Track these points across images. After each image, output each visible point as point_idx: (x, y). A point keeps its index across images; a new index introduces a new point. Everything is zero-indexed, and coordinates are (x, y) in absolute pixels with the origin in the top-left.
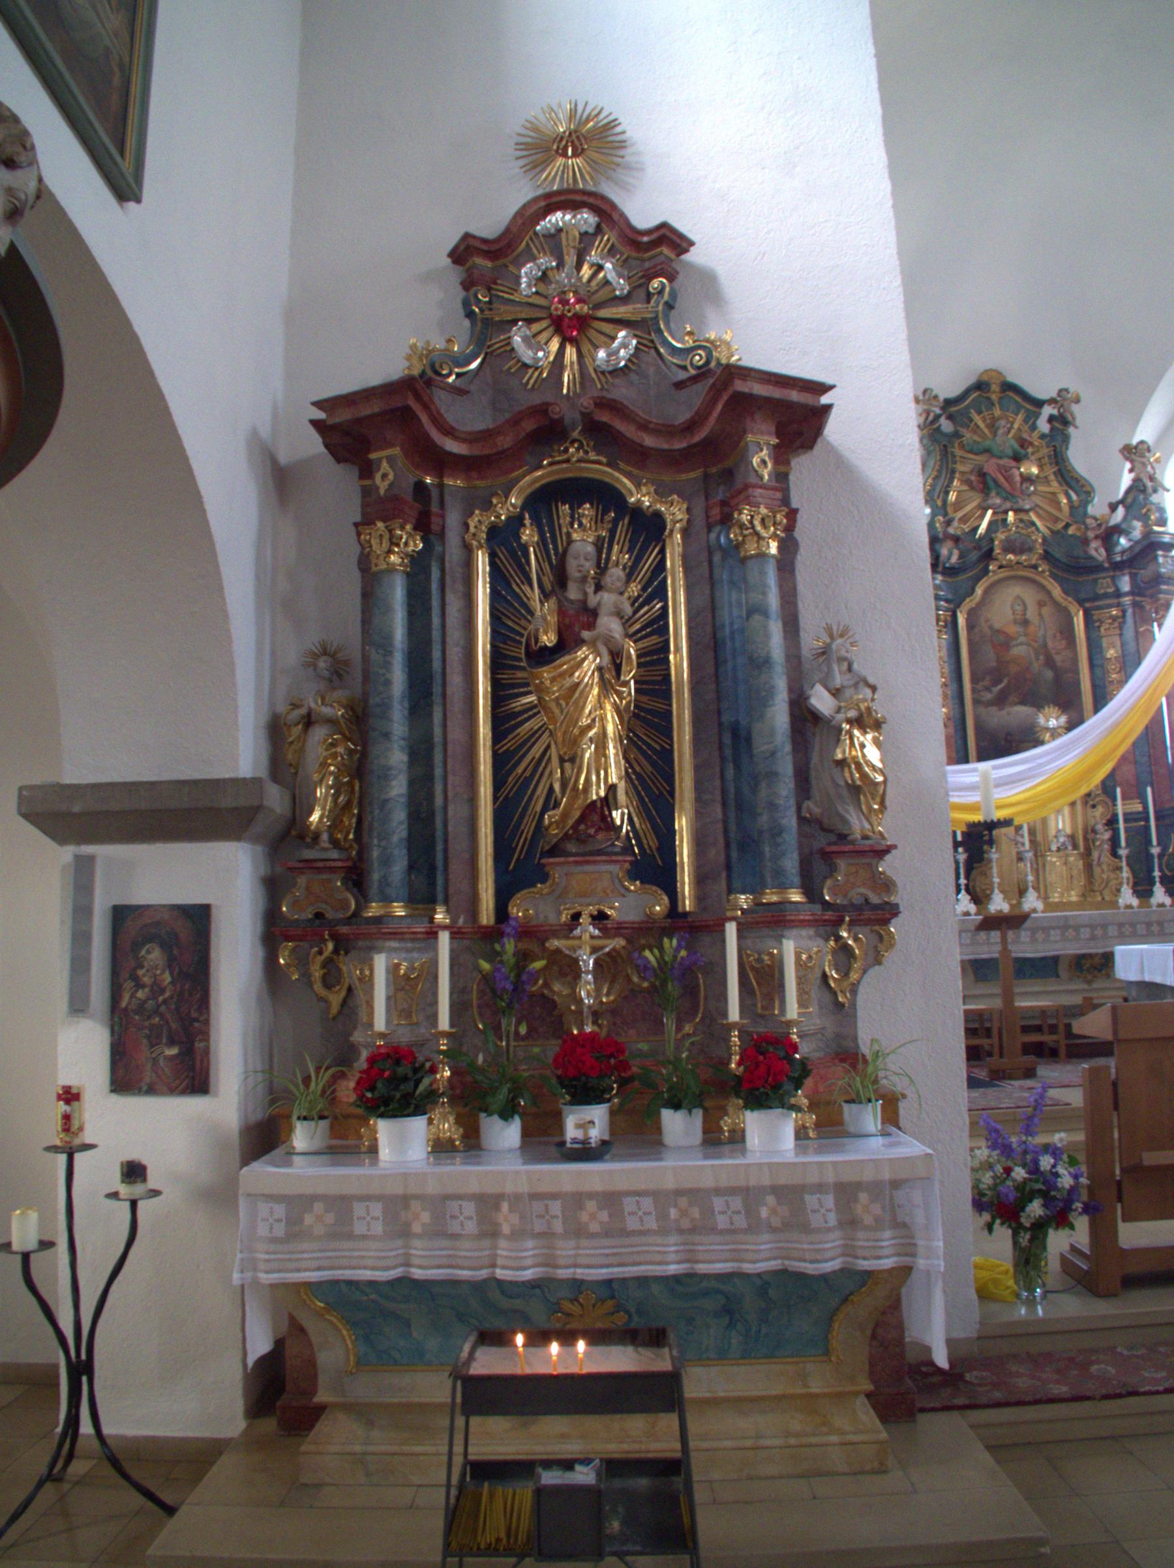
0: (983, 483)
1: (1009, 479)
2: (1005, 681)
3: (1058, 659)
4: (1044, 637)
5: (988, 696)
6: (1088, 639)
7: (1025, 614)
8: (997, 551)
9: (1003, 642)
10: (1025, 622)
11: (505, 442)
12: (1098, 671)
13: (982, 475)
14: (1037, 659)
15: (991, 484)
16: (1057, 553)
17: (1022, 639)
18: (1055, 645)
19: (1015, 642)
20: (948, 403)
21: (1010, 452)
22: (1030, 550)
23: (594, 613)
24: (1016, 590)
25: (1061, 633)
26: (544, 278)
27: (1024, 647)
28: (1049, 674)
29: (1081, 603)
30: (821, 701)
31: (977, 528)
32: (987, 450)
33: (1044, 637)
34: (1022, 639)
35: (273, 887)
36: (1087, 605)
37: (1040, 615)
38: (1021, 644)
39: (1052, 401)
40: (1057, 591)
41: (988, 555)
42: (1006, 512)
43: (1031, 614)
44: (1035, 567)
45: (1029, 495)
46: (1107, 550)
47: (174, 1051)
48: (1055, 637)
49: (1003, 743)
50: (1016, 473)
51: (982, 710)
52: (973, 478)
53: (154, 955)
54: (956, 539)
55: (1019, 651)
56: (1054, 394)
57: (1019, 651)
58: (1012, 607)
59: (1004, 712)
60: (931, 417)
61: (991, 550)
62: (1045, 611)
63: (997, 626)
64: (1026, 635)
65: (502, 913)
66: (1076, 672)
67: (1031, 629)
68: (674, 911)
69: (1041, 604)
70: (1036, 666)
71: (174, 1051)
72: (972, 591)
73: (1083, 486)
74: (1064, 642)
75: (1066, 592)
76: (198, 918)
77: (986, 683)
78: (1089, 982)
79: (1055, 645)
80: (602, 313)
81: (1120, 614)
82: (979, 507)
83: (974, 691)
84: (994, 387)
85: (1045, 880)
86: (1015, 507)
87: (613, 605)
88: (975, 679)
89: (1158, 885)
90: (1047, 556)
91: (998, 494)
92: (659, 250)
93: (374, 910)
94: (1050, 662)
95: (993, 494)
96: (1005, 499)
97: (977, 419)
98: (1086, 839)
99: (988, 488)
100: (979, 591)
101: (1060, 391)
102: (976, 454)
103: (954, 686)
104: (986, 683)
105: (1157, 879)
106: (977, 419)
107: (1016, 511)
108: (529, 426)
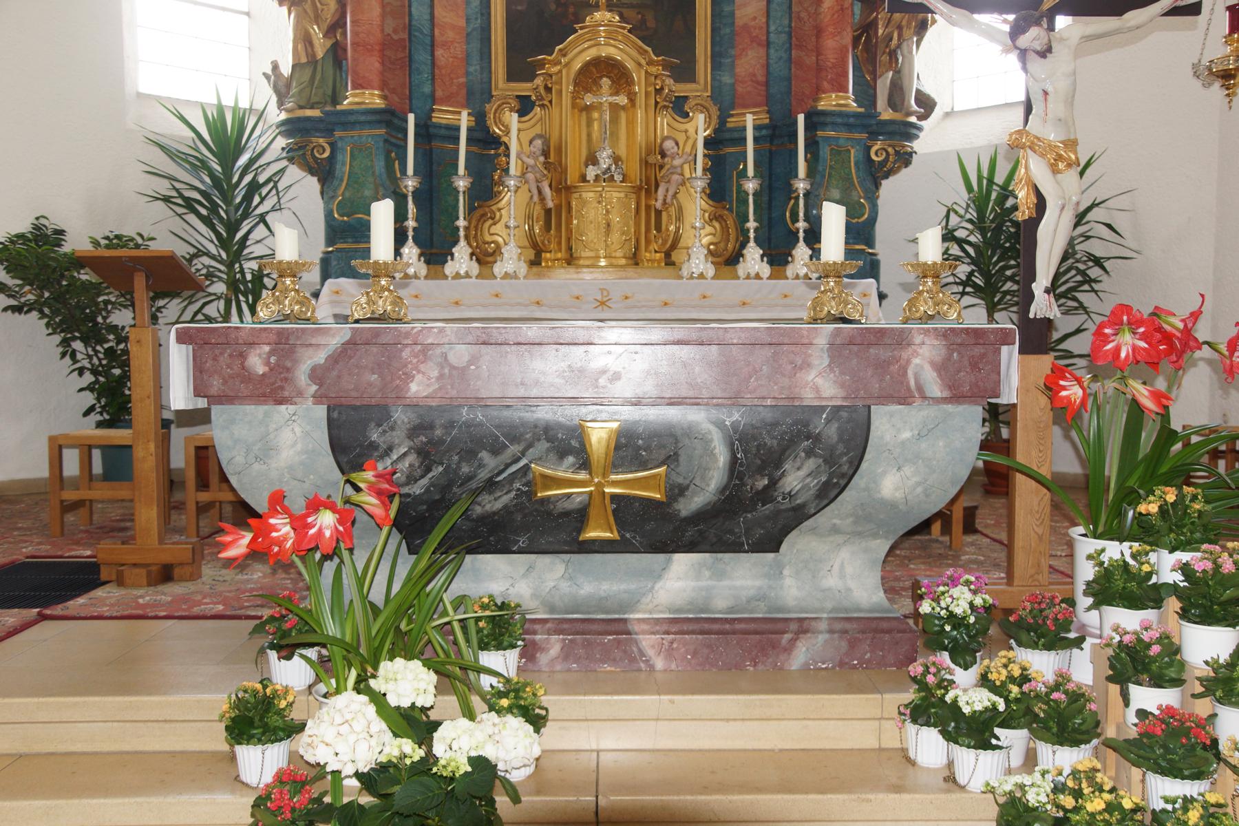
49: (553, 7)
85: (569, 231)
89: (752, 244)
98: (645, 164)
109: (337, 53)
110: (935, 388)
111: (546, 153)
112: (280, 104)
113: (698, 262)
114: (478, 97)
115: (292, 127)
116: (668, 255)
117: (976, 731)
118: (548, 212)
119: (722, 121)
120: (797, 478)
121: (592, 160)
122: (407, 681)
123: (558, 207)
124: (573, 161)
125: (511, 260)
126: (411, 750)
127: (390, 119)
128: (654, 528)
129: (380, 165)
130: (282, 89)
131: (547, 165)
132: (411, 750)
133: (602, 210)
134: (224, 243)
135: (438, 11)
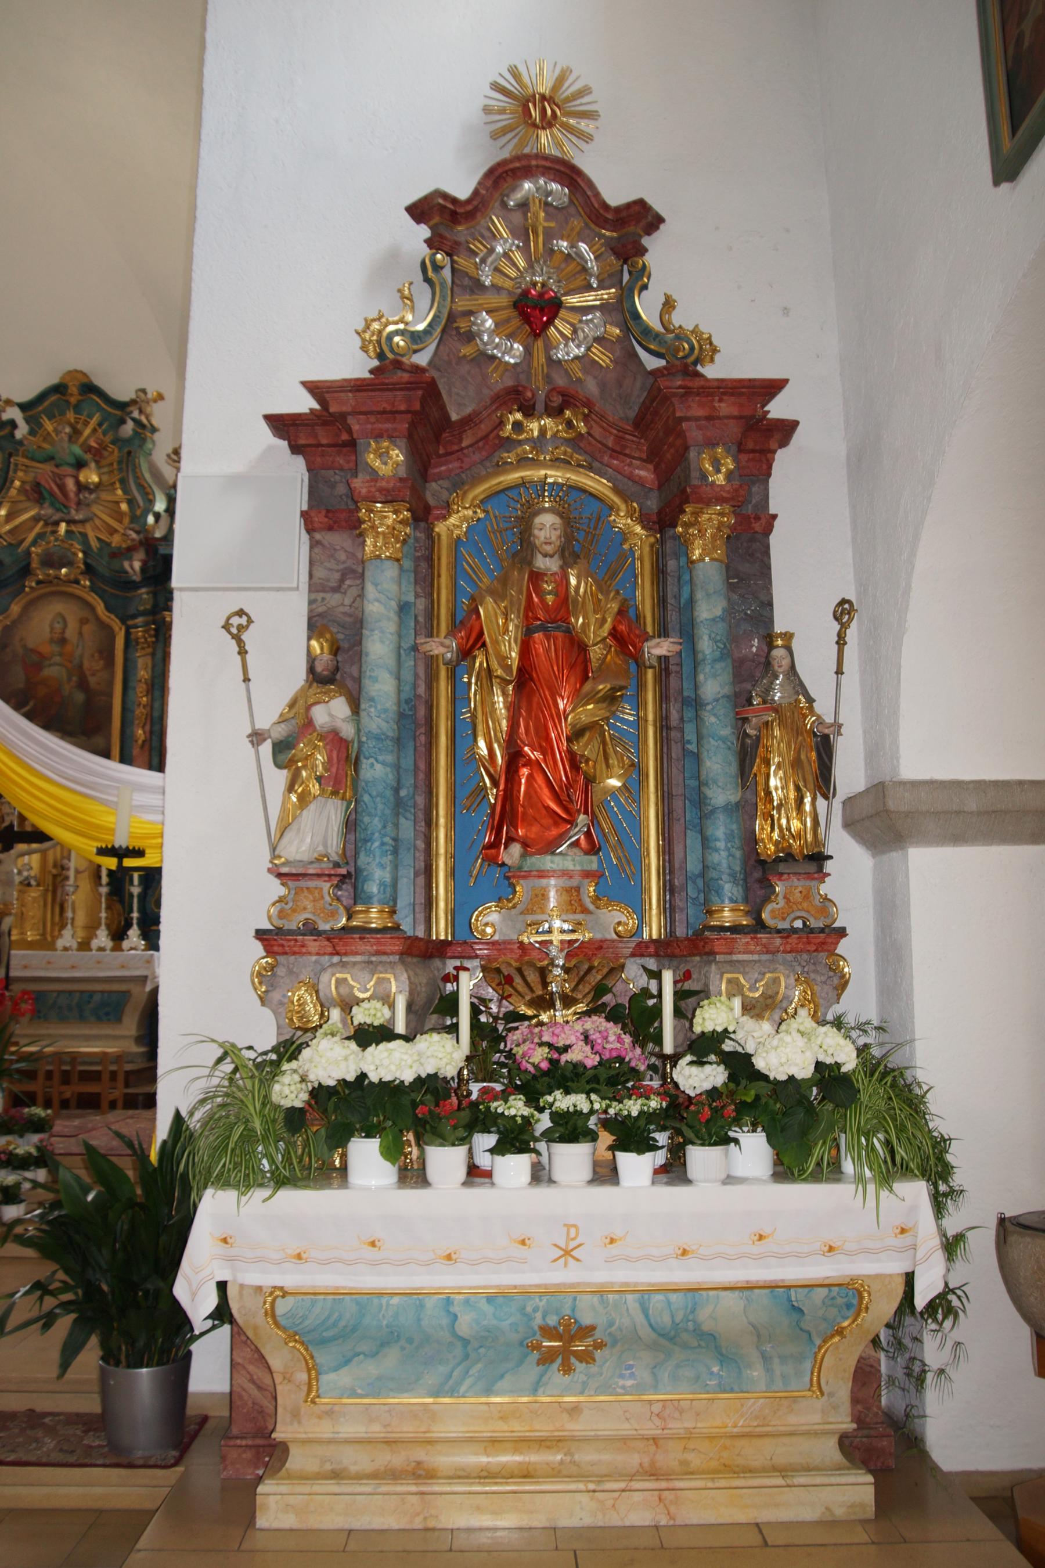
0: (37, 493)
1: (62, 488)
3: (92, 681)
4: (81, 657)
6: (126, 659)
7: (63, 632)
8: (34, 565)
10: (63, 641)
12: (130, 693)
13: (37, 487)
14: (69, 679)
15: (46, 494)
16: (102, 566)
17: (57, 659)
18: (92, 664)
19: (47, 662)
20: (24, 407)
21: (72, 460)
22: (69, 564)
24: (58, 607)
25: (100, 652)
27: (57, 668)
28: (80, 697)
29: (123, 621)
32: (51, 458)
33: (81, 657)
34: (57, 659)
36: (130, 622)
37: (80, 634)
38: (56, 664)
39: (133, 402)
40: (100, 608)
41: (26, 571)
42: (57, 524)
43: (71, 633)
44: (77, 582)
45: (88, 505)
48: (93, 656)
50: (70, 484)
52: (28, 488)
55: (53, 671)
56: (134, 396)
57: (53, 671)
61: (29, 564)
62: (86, 628)
63: (31, 645)
64: (61, 654)
66: (110, 695)
67: (68, 648)
69: (83, 621)
70: (66, 689)
73: (147, 494)
74: (102, 662)
75: (108, 608)
79: (92, 664)
81: (152, 632)
84: (73, 390)
86: (67, 518)
90: (89, 570)
91: (52, 505)
94: (83, 684)
95: (46, 505)
96: (58, 510)
97: (49, 426)
99: (44, 499)
100: (15, 609)
101: (137, 391)
102: (39, 462)
105: (135, 921)
106: (49, 426)
107: (68, 522)
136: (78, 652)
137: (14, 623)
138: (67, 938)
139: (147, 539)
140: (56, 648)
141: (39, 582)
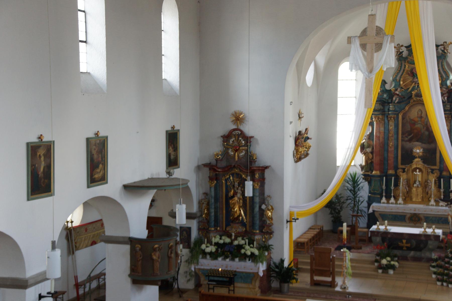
2: (412, 135)
5: (406, 139)
8: (413, 96)
9: (413, 123)
10: (421, 117)
11: (226, 169)
17: (420, 122)
23: (237, 192)
26: (233, 141)
28: (427, 133)
30: (263, 207)
31: (409, 88)
34: (420, 122)
35: (199, 222)
39: (441, 45)
41: (410, 97)
46: (447, 98)
47: (187, 244)
51: (404, 143)
53: (185, 233)
54: (398, 95)
55: (418, 126)
56: (442, 43)
57: (418, 126)
58: (418, 113)
59: (411, 144)
60: (399, 53)
61: (411, 96)
63: (412, 117)
64: (421, 121)
65: (226, 229)
67: (423, 119)
68: (246, 230)
70: (423, 131)
71: (187, 244)
72: (404, 109)
76: (190, 229)
77: (406, 135)
78: (415, 224)
80: (241, 148)
82: (411, 81)
83: (402, 137)
87: (239, 191)
88: (403, 134)
92: (248, 140)
93: (210, 229)
100: (407, 108)
101: (444, 43)
103: (396, 136)
104: (406, 135)
108: (229, 167)
109: (372, 163)
110: (433, 239)
111: (407, 182)
112: (362, 170)
113: (432, 202)
114: (396, 168)
115: (364, 175)
116: (429, 199)
117: (434, 267)
118: (407, 192)
119: (441, 174)
120: (422, 246)
121: (415, 182)
122: (389, 259)
123: (409, 190)
124: (411, 182)
125: (400, 201)
126: (389, 263)
127: (381, 177)
128: (409, 249)
129: (379, 184)
130: (362, 167)
131: (407, 184)
132: (389, 263)
133: (417, 191)
134: (354, 195)
135: (389, 155)
136: (426, 121)
137: (406, 112)
138: (432, 202)
139: (449, 90)
140: (419, 119)
141: (414, 101)
